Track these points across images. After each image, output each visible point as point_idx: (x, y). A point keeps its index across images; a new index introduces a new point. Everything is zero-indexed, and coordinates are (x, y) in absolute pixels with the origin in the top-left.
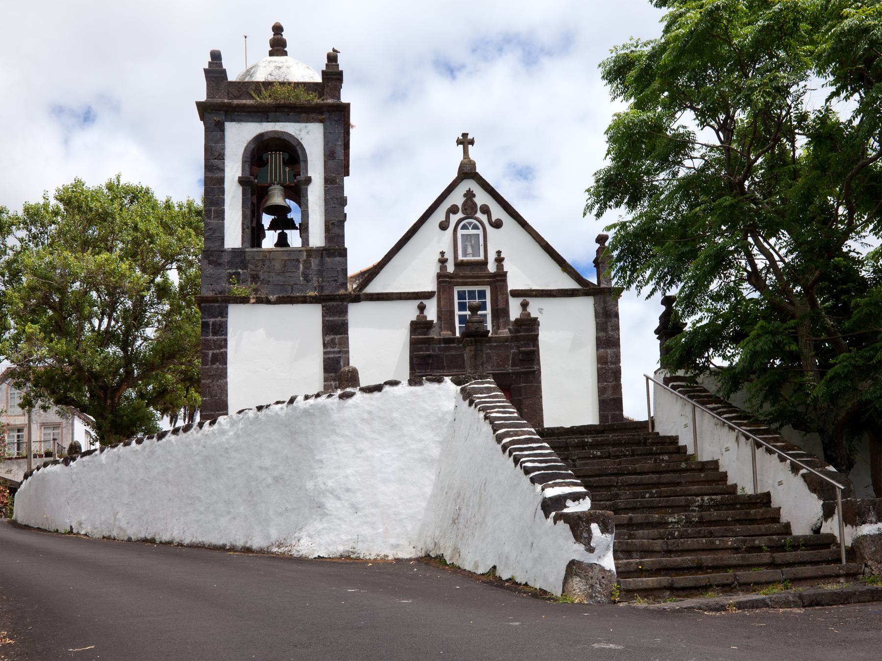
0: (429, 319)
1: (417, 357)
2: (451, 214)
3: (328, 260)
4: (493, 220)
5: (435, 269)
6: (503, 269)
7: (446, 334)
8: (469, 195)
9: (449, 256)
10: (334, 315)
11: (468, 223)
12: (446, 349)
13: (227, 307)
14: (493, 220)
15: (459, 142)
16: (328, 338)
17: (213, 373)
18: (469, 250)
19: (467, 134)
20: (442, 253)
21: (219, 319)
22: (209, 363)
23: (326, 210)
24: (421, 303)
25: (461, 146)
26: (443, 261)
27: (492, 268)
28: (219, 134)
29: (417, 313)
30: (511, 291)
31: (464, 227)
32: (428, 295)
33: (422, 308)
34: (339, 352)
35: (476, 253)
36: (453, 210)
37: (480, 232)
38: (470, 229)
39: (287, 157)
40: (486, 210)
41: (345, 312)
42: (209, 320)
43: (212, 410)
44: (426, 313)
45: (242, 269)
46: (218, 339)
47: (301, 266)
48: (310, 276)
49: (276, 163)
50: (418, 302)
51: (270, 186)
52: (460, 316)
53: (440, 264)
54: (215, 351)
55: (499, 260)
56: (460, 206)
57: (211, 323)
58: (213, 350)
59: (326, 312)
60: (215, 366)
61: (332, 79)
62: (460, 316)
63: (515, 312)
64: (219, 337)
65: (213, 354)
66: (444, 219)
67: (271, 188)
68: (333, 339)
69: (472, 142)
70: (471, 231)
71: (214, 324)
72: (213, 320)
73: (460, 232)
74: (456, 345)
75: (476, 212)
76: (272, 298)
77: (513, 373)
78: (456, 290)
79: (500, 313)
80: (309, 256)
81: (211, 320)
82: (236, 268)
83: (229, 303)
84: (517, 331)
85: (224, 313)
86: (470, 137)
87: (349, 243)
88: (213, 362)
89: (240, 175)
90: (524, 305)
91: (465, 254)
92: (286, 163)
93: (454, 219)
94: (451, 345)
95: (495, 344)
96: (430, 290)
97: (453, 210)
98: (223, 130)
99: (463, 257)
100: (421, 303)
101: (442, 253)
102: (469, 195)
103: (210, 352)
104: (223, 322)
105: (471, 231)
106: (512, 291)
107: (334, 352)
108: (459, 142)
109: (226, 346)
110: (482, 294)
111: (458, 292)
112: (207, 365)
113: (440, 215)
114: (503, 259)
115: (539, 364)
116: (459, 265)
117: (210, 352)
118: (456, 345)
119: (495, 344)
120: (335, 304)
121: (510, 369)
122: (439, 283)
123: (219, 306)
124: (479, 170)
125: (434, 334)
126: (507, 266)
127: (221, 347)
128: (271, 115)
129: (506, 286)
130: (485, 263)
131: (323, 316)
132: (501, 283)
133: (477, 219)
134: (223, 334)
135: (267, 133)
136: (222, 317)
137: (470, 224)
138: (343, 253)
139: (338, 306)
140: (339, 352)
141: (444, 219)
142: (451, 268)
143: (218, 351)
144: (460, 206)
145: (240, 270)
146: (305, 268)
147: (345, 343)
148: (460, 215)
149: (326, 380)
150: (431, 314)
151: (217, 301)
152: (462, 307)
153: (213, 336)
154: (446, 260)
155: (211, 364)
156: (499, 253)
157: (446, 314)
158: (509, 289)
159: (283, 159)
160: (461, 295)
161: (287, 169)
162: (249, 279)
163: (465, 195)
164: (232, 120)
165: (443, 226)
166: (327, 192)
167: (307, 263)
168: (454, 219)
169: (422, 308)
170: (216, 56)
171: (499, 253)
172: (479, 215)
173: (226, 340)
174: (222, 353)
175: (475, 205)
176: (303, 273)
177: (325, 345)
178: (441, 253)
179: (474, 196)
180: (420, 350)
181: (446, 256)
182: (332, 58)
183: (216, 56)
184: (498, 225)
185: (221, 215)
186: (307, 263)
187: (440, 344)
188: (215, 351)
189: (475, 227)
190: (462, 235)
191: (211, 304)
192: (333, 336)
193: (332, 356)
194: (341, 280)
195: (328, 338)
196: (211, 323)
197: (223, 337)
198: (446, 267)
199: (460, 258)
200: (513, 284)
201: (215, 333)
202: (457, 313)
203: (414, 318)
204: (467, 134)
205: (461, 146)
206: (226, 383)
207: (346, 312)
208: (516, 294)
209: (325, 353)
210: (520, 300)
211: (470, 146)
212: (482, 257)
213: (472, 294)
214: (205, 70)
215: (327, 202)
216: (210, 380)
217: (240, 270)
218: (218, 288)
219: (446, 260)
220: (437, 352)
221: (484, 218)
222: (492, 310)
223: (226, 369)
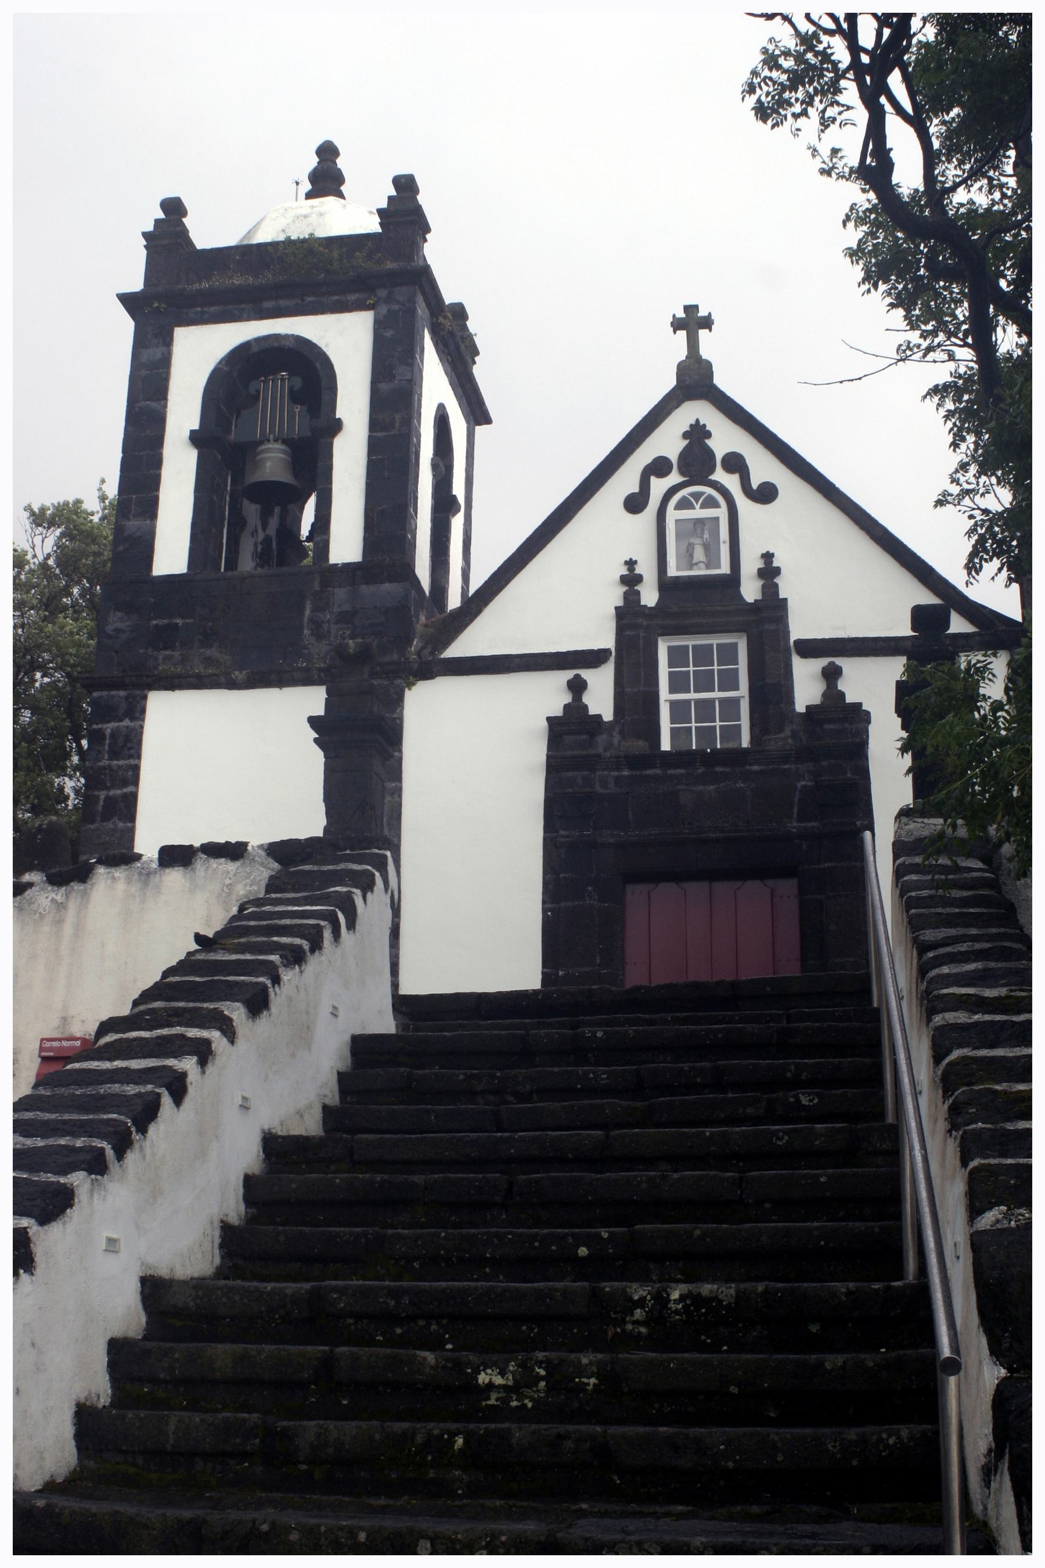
0: (593, 711)
2: (653, 479)
3: (365, 589)
4: (755, 486)
5: (615, 596)
6: (777, 593)
7: (640, 746)
8: (697, 434)
9: (647, 569)
11: (693, 495)
13: (145, 698)
14: (755, 486)
15: (677, 325)
18: (699, 554)
19: (696, 307)
21: (127, 722)
22: (99, 819)
23: (368, 484)
24: (577, 676)
25: (682, 334)
26: (631, 580)
27: (750, 590)
28: (164, 349)
30: (796, 642)
31: (684, 504)
32: (593, 658)
33: (577, 687)
35: (712, 558)
37: (722, 513)
38: (698, 506)
39: (298, 382)
40: (735, 463)
42: (105, 726)
44: (587, 699)
45: (182, 617)
46: (120, 767)
48: (325, 626)
49: (274, 398)
51: (262, 443)
52: (673, 704)
53: (625, 589)
54: (112, 793)
55: (769, 572)
56: (674, 458)
57: (108, 732)
58: (109, 789)
60: (110, 825)
64: (121, 763)
65: (108, 798)
66: (636, 490)
67: (263, 447)
69: (707, 323)
70: (699, 512)
73: (672, 515)
74: (658, 771)
75: (712, 469)
76: (239, 675)
80: (325, 583)
81: (109, 727)
83: (151, 690)
85: (137, 712)
86: (702, 313)
88: (106, 816)
89: (196, 427)
90: (831, 675)
91: (687, 558)
92: (295, 397)
93: (659, 486)
94: (649, 772)
95: (756, 768)
97: (659, 467)
99: (678, 569)
100: (577, 676)
101: (631, 564)
102: (697, 434)
104: (133, 729)
105: (699, 512)
106: (798, 643)
108: (677, 325)
109: (136, 781)
110: (728, 654)
111: (671, 650)
112: (93, 822)
114: (777, 571)
116: (667, 586)
117: (102, 795)
118: (658, 771)
119: (756, 768)
121: (794, 826)
122: (620, 630)
123: (127, 698)
124: (721, 381)
126: (786, 588)
127: (125, 783)
129: (787, 633)
130: (734, 579)
132: (772, 627)
134: (131, 756)
135: (258, 340)
136: (132, 719)
137: (697, 496)
141: (636, 489)
142: (649, 596)
143: (118, 792)
144: (674, 458)
145: (179, 621)
148: (675, 478)
152: (678, 683)
153: (110, 759)
154: (639, 579)
155: (103, 821)
156: (768, 557)
158: (794, 636)
159: (291, 389)
160: (677, 656)
161: (298, 409)
163: (686, 435)
165: (635, 504)
168: (659, 486)
169: (577, 687)
170: (174, 208)
171: (768, 557)
172: (719, 475)
174: (125, 796)
175: (710, 454)
176: (311, 620)
178: (626, 563)
179: (708, 435)
181: (638, 570)
182: (405, 186)
183: (174, 208)
184: (766, 494)
187: (618, 769)
188: (112, 793)
189: (710, 503)
191: (113, 693)
196: (108, 732)
197: (132, 762)
198: (638, 593)
199: (672, 571)
200: (799, 629)
201: (114, 754)
202: (665, 694)
203: (557, 711)
204: (696, 307)
205: (682, 334)
207: (399, 700)
208: (810, 649)
210: (817, 665)
211: (703, 333)
212: (725, 568)
213: (703, 655)
214: (145, 235)
217: (179, 621)
219: (639, 579)
221: (731, 482)
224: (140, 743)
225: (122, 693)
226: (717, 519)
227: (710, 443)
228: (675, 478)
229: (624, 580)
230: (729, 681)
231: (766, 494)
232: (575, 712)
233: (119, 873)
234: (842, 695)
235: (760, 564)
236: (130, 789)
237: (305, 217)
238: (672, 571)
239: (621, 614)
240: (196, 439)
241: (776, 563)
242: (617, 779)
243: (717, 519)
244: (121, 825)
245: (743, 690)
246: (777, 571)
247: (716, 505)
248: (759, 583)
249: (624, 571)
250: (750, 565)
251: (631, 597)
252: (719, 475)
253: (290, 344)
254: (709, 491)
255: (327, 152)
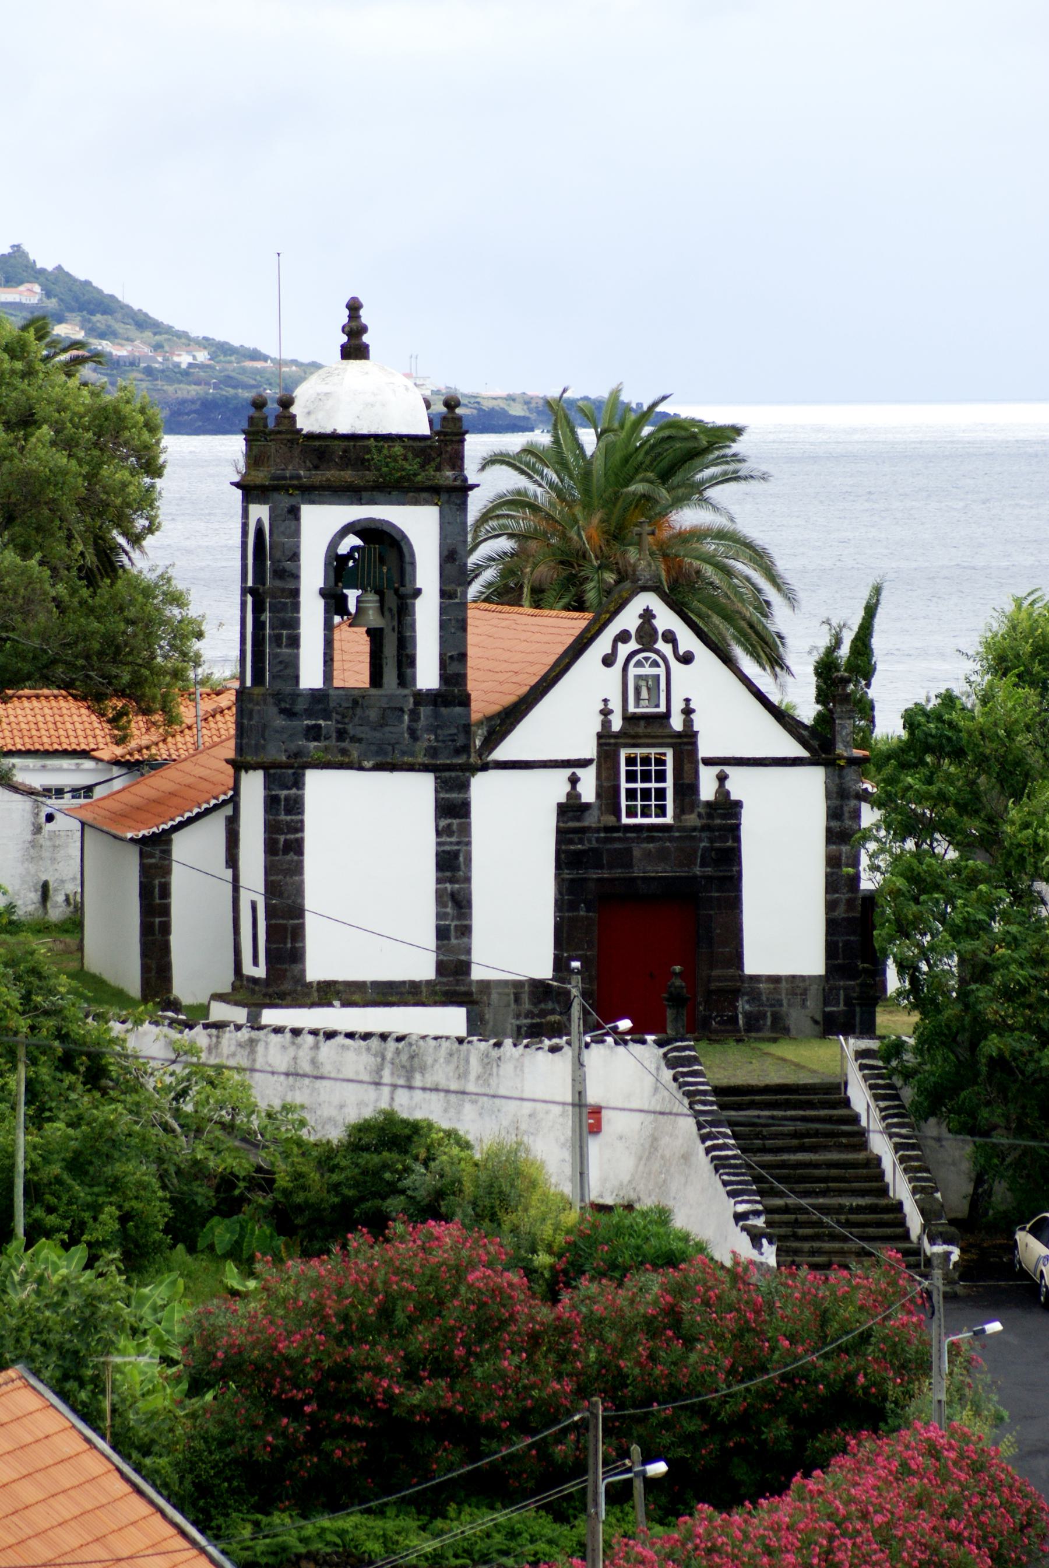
0: (584, 799)
1: (566, 852)
2: (620, 645)
3: (444, 710)
4: (681, 652)
7: (609, 820)
8: (647, 616)
9: (616, 705)
10: (450, 790)
12: (607, 840)
13: (304, 775)
14: (681, 652)
16: (443, 823)
17: (285, 866)
20: (605, 701)
21: (294, 791)
23: (441, 637)
24: (574, 774)
26: (606, 712)
27: (677, 723)
28: (295, 522)
29: (568, 787)
31: (639, 664)
32: (584, 763)
33: (574, 781)
34: (458, 843)
36: (623, 637)
37: (661, 671)
40: (670, 637)
41: (465, 786)
43: (283, 918)
44: (580, 787)
47: (406, 717)
50: (568, 772)
52: (628, 790)
55: (688, 711)
56: (633, 632)
59: (441, 786)
60: (288, 857)
61: (452, 441)
62: (628, 790)
63: (707, 790)
65: (286, 841)
68: (449, 825)
71: (287, 798)
72: (285, 792)
73: (633, 671)
75: (655, 641)
76: (367, 764)
77: (701, 877)
78: (623, 754)
79: (687, 789)
80: (417, 703)
81: (283, 793)
82: (317, 719)
84: (710, 816)
85: (298, 783)
87: (471, 686)
90: (722, 778)
93: (624, 650)
96: (588, 756)
97: (623, 637)
98: (297, 518)
100: (574, 774)
102: (647, 616)
103: (282, 838)
107: (451, 843)
109: (301, 829)
112: (277, 855)
113: (602, 645)
114: (693, 711)
115: (740, 864)
116: (629, 719)
117: (282, 838)
119: (677, 834)
120: (453, 774)
121: (697, 870)
122: (600, 745)
125: (591, 820)
128: (365, 495)
130: (667, 715)
131: (436, 791)
133: (657, 652)
137: (646, 659)
138: (465, 701)
139: (458, 777)
140: (458, 843)
141: (609, 651)
142: (617, 724)
144: (633, 632)
145: (321, 722)
146: (411, 720)
147: (466, 830)
148: (633, 645)
149: (439, 881)
150: (588, 792)
151: (292, 767)
152: (631, 777)
154: (611, 712)
157: (608, 791)
162: (334, 735)
163: (641, 616)
164: (312, 502)
165: (608, 661)
166: (443, 610)
167: (414, 715)
169: (574, 781)
172: (661, 645)
173: (302, 821)
177: (438, 833)
179: (654, 617)
180: (571, 842)
181: (610, 706)
184: (687, 659)
185: (294, 642)
186: (414, 715)
189: (655, 664)
190: (638, 677)
192: (449, 821)
193: (447, 848)
194: (460, 742)
195: (443, 823)
197: (299, 817)
198: (610, 722)
200: (705, 750)
201: (288, 812)
202: (624, 785)
203: (563, 799)
206: (302, 882)
208: (709, 762)
209: (438, 844)
210: (716, 770)
212: (662, 709)
213: (646, 761)
215: (443, 626)
216: (280, 877)
217: (321, 722)
218: (293, 747)
219: (611, 712)
220: (594, 844)
221: (666, 648)
222: (675, 785)
223: (302, 862)
224: (303, 804)
225: (290, 771)
226: (658, 676)
227: (655, 622)
228: (633, 645)
229: (602, 712)
230: (661, 777)
231: (687, 659)
232: (573, 795)
233: (600, 1046)
234: (728, 793)
235: (683, 706)
236: (298, 835)
237: (372, 405)
238: (632, 709)
239: (599, 736)
240: (323, 593)
241: (692, 706)
242: (598, 839)
243: (658, 676)
244: (296, 858)
245: (669, 785)
246: (693, 711)
247: (658, 666)
248: (683, 717)
249: (602, 706)
250: (677, 706)
251: (606, 724)
252: (661, 645)
253: (386, 528)
254: (654, 656)
255: (354, 307)
